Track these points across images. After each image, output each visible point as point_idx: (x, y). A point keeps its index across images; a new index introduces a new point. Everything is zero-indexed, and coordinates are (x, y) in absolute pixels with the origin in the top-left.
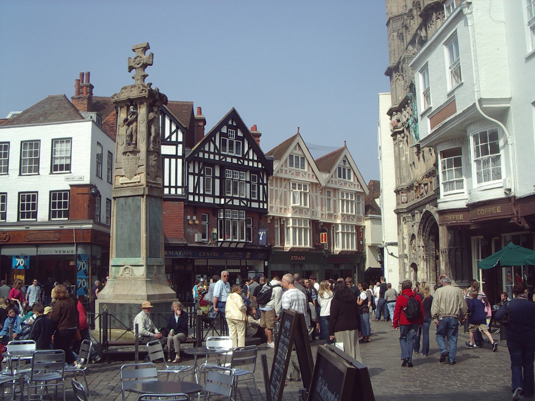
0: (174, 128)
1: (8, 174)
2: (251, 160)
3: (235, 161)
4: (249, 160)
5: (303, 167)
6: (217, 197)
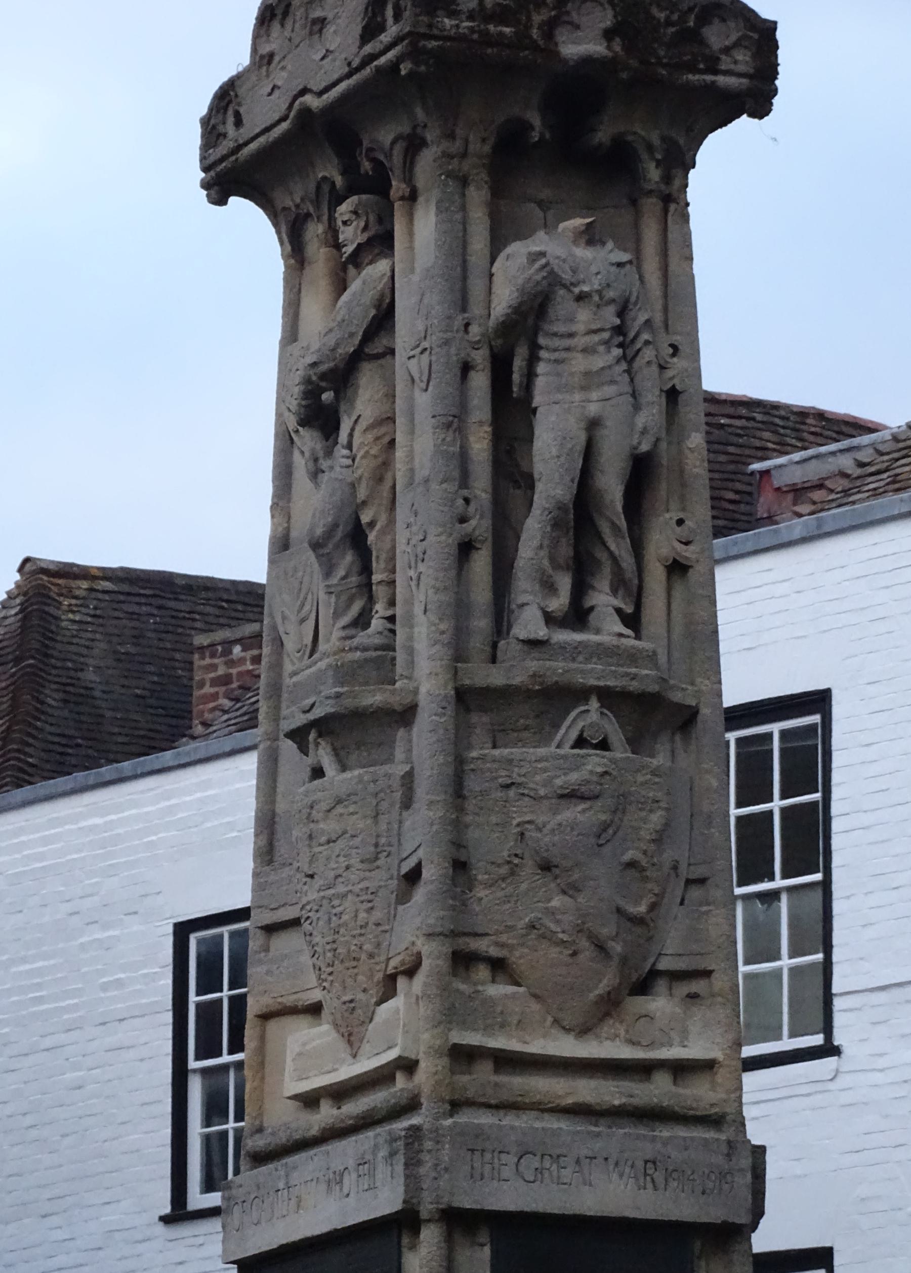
1: (829, 1050)
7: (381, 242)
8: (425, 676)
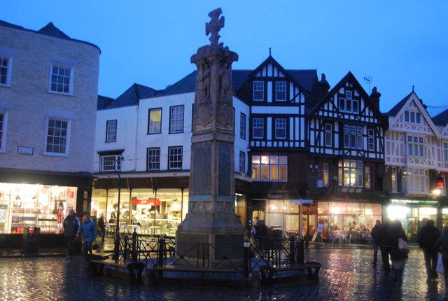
0: (297, 92)
2: (367, 117)
3: (352, 118)
4: (365, 117)
5: (419, 121)
6: (337, 149)
7: (209, 67)
8: (214, 99)
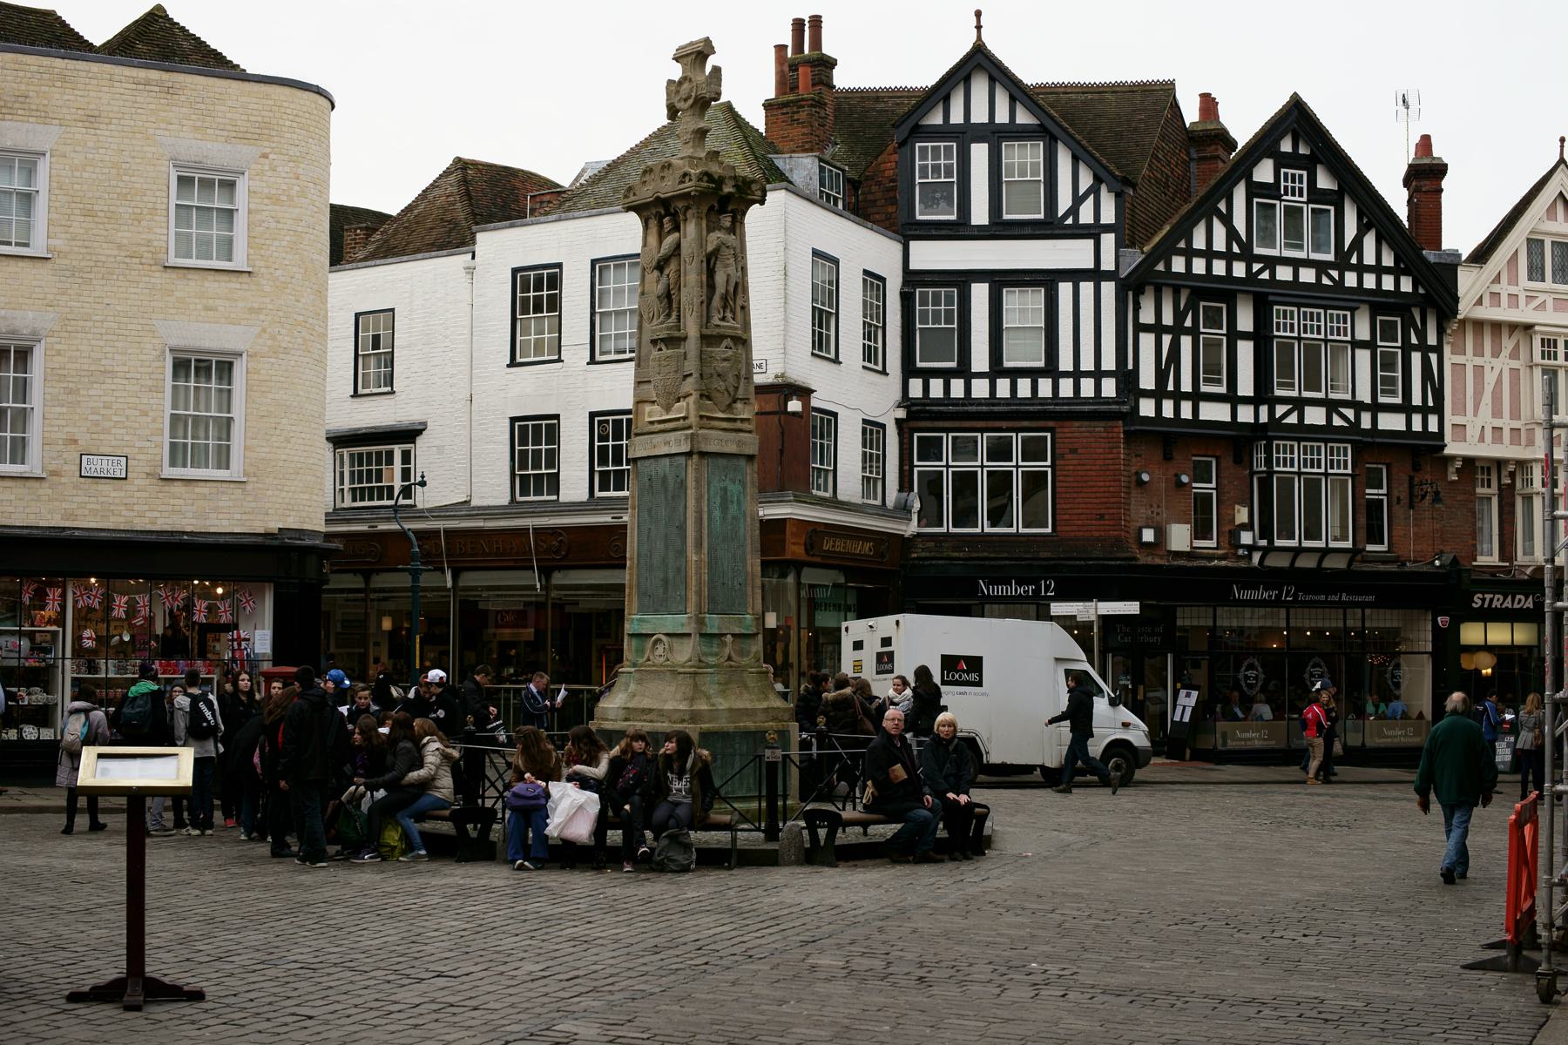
7: (677, 228)
8: (692, 328)
